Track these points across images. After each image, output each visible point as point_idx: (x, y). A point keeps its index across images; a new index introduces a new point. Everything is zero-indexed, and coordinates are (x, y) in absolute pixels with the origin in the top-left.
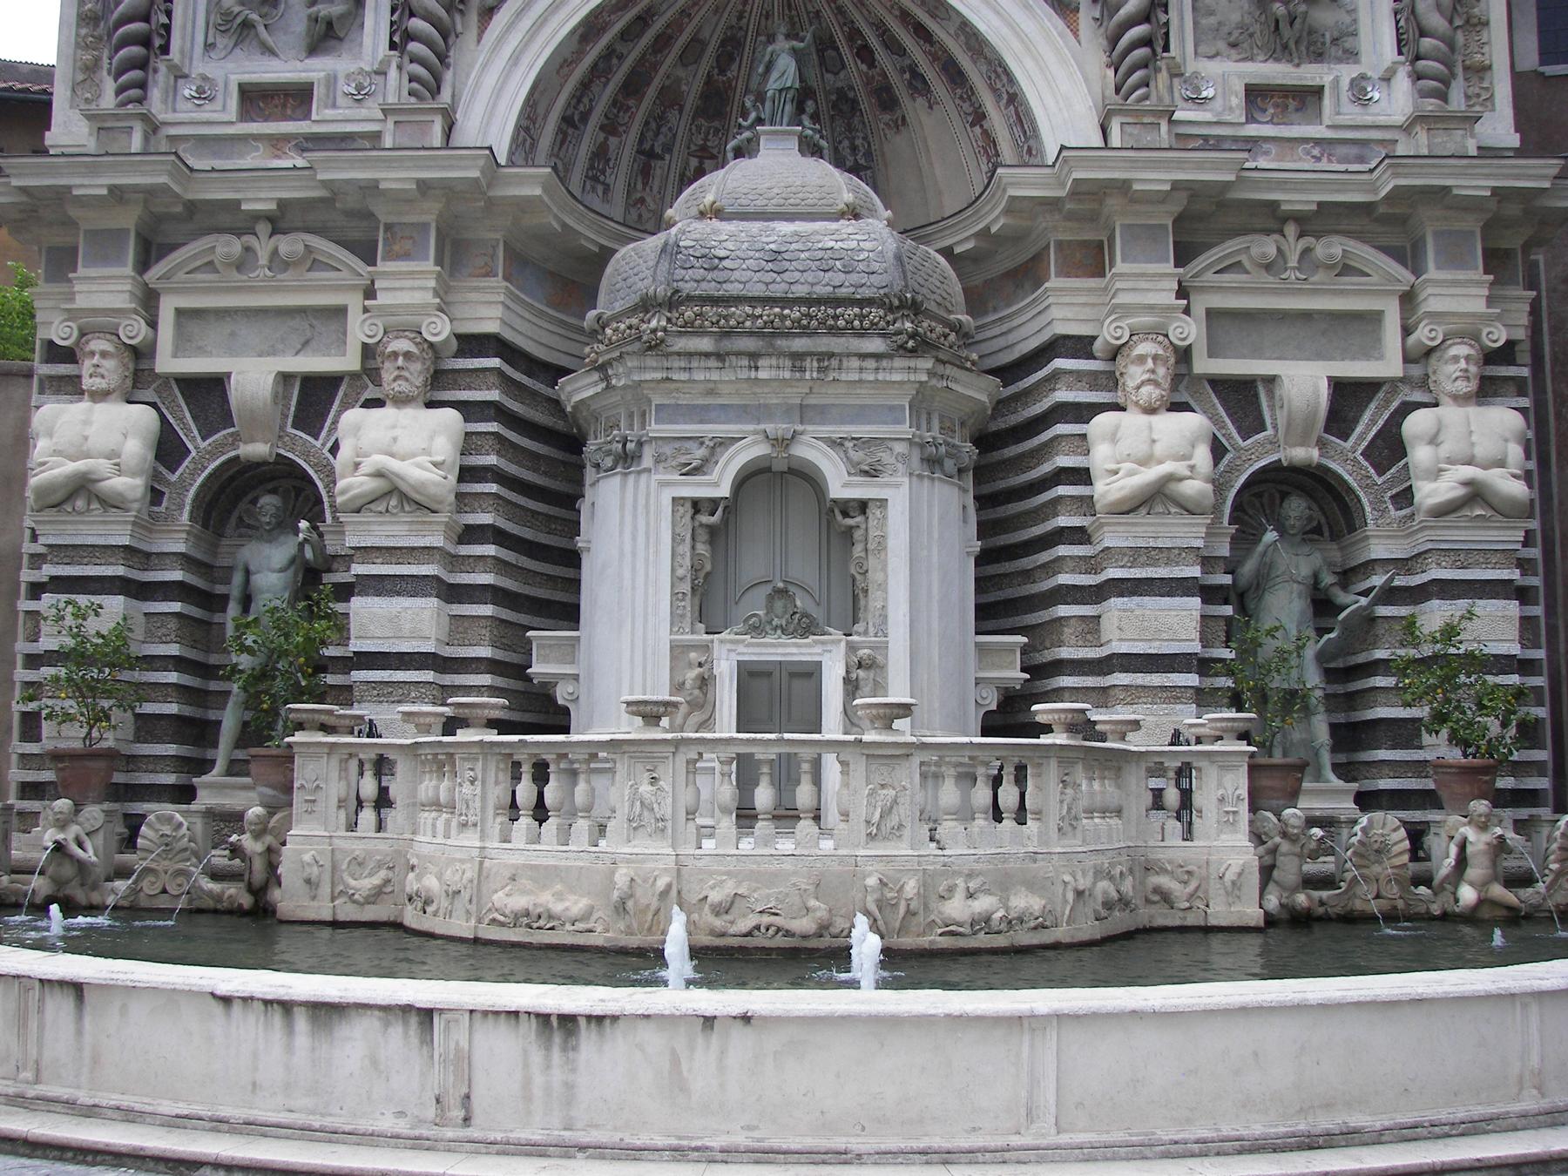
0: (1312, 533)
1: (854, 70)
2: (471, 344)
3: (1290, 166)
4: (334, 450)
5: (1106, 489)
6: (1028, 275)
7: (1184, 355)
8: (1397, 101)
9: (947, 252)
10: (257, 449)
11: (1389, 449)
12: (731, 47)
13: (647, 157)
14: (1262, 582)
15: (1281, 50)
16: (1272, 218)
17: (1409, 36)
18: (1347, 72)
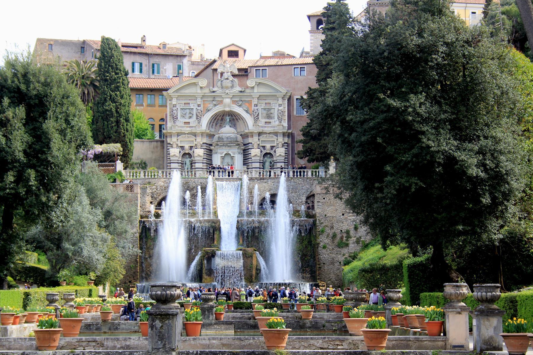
0: (270, 158)
1: (234, 117)
2: (203, 143)
3: (268, 129)
4: (193, 152)
5: (252, 155)
6: (248, 137)
7: (259, 144)
8: (277, 123)
9: (241, 135)
10: (187, 152)
11: (275, 152)
12: (223, 115)
13: (216, 124)
14: (266, 161)
15: (268, 119)
16: (266, 133)
17: (278, 117)
18: (274, 120)
